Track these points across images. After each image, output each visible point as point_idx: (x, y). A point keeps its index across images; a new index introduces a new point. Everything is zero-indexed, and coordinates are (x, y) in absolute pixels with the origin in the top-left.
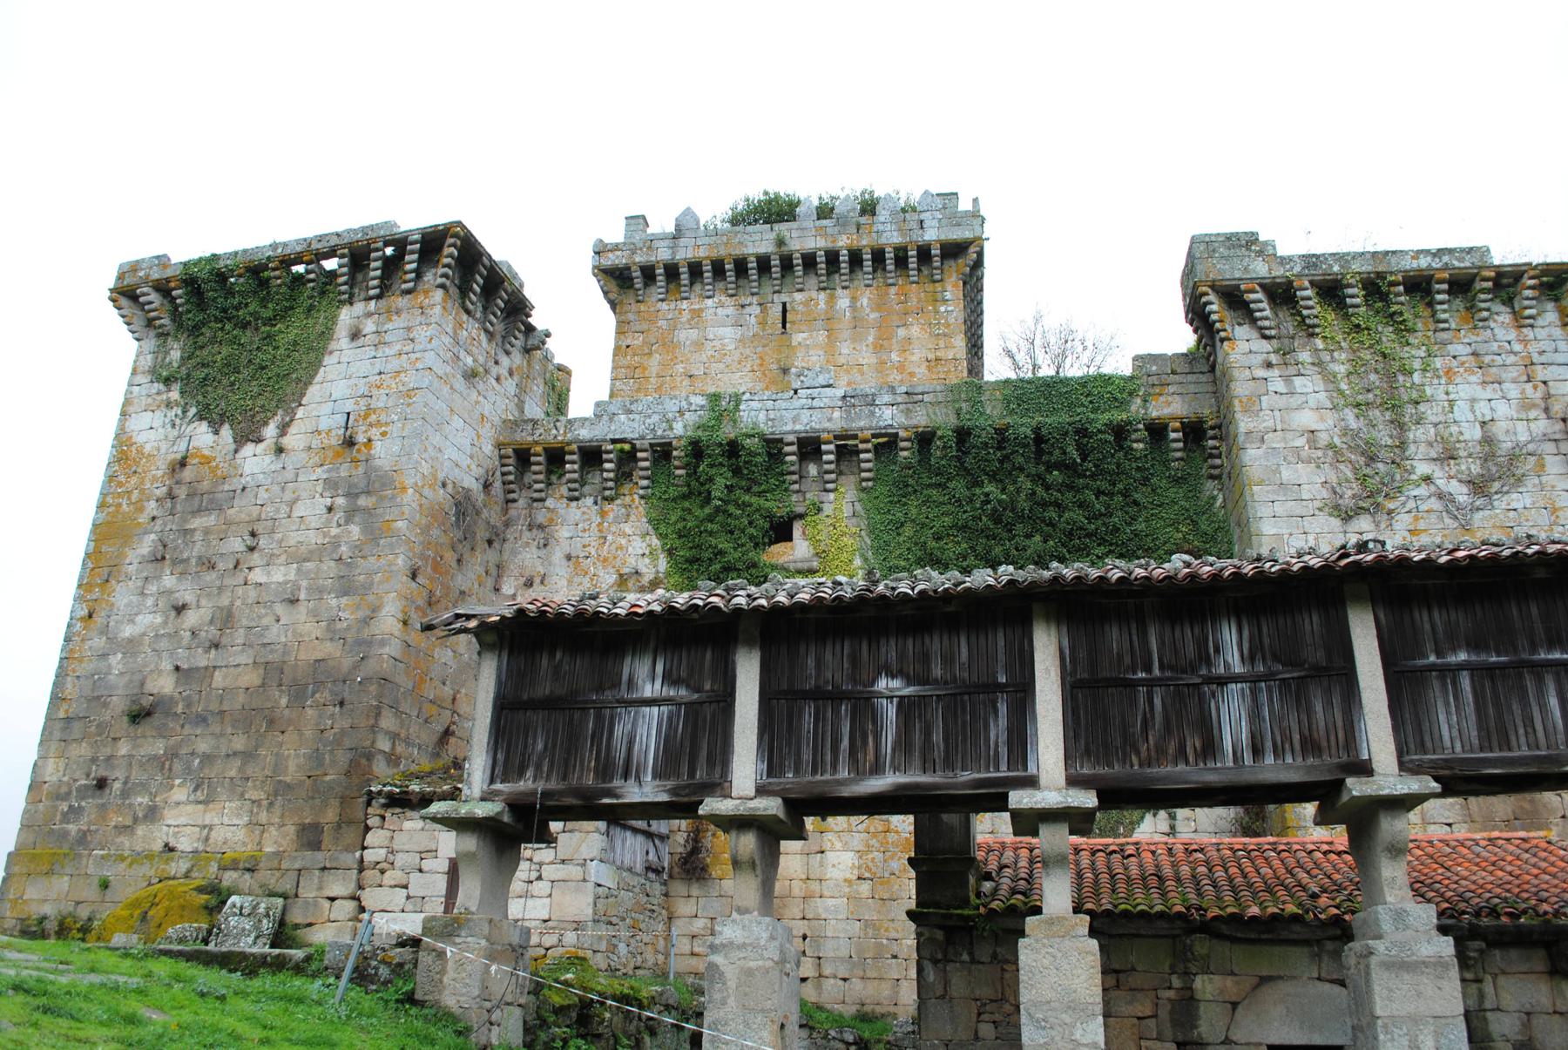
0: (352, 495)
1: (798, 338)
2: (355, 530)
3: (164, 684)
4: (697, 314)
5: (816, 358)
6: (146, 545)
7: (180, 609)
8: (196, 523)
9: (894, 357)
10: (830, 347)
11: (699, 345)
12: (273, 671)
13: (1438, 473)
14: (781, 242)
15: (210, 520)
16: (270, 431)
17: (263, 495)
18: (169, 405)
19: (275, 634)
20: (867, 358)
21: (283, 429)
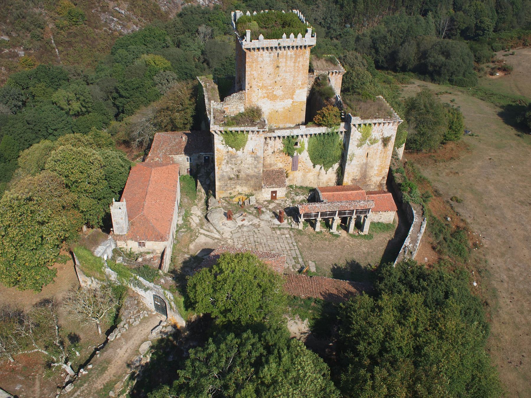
0: (255, 158)
1: (280, 60)
2: (256, 162)
3: (233, 176)
4: (262, 55)
5: (283, 64)
6: (225, 161)
7: (233, 169)
8: (232, 159)
9: (297, 64)
10: (286, 62)
11: (262, 61)
12: (248, 176)
13: (369, 142)
14: (279, 44)
15: (235, 159)
16: (241, 149)
17: (242, 157)
18: (223, 144)
19: (247, 172)
20: (292, 64)
21: (243, 150)
